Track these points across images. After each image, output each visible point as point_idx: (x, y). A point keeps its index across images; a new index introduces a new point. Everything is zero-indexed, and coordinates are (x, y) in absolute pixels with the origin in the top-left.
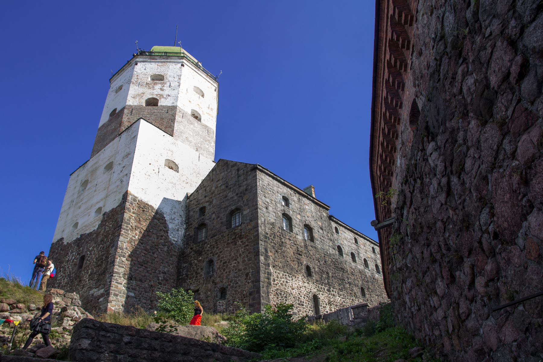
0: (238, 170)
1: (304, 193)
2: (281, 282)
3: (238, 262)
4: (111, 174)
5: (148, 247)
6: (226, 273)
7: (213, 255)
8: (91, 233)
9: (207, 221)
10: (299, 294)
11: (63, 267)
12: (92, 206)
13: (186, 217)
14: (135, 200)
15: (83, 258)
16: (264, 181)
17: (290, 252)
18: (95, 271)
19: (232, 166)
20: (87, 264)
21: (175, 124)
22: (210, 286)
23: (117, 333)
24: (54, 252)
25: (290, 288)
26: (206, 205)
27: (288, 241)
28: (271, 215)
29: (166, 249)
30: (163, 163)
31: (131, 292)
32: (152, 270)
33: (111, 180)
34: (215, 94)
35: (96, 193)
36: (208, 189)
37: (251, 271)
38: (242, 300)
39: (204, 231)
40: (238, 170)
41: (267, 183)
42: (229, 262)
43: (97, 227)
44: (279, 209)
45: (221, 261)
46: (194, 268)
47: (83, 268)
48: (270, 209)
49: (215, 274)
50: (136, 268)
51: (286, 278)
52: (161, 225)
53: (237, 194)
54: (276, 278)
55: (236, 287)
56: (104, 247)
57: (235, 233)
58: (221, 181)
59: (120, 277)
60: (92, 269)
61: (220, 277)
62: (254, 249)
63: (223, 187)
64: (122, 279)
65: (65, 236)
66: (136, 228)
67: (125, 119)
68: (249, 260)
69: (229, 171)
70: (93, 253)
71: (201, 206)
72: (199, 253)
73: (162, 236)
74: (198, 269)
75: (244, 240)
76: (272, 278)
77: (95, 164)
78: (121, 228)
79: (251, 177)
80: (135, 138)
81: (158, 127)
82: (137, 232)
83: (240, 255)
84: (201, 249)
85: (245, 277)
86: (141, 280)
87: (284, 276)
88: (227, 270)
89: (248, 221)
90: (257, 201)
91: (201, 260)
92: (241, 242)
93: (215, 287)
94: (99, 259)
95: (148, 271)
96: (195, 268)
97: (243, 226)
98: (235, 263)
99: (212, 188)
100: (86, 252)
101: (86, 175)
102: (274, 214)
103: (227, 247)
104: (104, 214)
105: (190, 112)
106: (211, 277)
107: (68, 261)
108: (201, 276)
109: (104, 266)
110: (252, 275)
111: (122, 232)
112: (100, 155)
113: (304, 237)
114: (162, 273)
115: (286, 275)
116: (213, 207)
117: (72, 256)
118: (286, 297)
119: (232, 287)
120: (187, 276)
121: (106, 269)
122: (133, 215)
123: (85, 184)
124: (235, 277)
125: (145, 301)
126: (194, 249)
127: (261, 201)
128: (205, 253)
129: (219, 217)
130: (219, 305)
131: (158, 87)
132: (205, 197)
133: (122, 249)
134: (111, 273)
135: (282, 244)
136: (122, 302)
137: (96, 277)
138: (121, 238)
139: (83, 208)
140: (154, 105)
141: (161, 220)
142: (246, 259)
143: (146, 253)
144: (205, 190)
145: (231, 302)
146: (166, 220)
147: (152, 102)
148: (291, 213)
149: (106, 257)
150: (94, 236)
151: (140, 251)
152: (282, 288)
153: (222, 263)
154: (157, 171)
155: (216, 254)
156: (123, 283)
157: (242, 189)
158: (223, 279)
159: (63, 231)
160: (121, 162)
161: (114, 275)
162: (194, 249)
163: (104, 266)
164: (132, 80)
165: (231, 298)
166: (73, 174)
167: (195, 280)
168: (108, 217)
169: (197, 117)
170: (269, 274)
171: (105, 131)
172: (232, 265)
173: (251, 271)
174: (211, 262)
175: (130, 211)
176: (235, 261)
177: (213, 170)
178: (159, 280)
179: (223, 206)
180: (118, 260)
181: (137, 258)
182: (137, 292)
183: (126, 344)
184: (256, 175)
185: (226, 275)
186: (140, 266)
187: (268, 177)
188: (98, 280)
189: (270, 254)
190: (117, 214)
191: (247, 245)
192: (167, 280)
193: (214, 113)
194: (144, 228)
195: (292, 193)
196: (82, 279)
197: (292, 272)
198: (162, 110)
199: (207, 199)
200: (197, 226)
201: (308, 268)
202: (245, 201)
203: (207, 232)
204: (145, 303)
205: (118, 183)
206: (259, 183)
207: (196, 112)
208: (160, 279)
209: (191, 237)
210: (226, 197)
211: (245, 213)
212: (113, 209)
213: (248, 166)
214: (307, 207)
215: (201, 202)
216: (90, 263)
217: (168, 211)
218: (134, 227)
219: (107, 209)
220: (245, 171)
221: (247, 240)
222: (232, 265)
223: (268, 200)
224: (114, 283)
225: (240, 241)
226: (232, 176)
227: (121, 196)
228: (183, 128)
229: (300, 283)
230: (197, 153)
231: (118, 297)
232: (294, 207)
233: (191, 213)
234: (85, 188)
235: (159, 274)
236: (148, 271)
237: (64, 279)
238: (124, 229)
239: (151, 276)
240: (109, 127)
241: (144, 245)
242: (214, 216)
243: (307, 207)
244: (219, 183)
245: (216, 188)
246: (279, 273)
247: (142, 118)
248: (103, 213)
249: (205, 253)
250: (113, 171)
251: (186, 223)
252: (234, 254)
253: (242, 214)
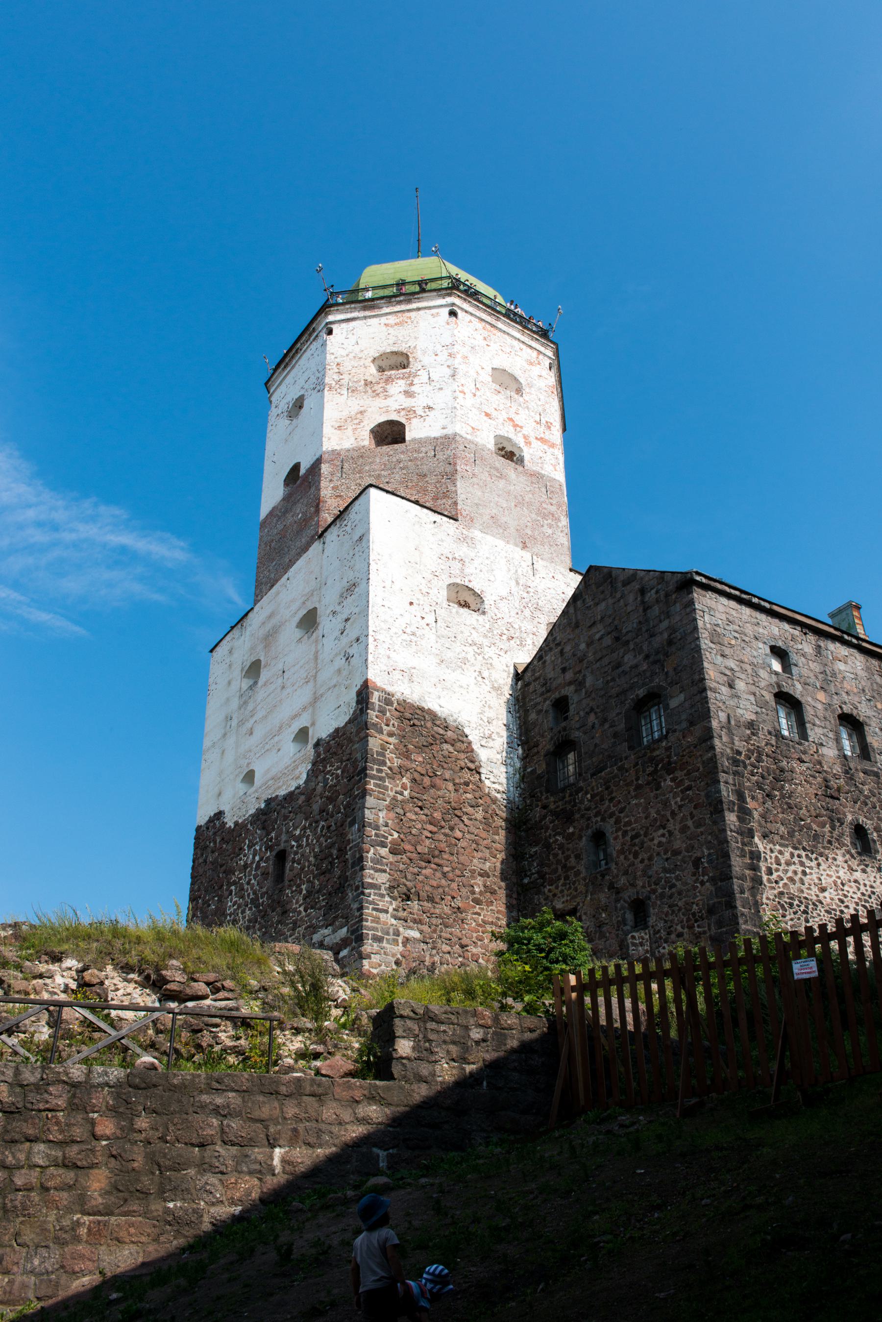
0: (643, 591)
1: (832, 630)
2: (790, 874)
3: (671, 833)
4: (317, 641)
5: (437, 815)
6: (642, 861)
7: (603, 820)
8: (291, 794)
9: (576, 735)
10: (842, 901)
11: (235, 883)
12: (281, 728)
13: (520, 727)
14: (388, 702)
15: (281, 857)
16: (712, 612)
17: (804, 790)
18: (317, 887)
19: (626, 583)
20: (295, 872)
21: (458, 484)
22: (603, 897)
23: (458, 1025)
24: (206, 847)
25: (815, 889)
26: (569, 691)
27: (795, 764)
28: (742, 703)
29: (479, 815)
30: (441, 595)
31: (411, 928)
32: (453, 869)
33: (320, 657)
34: (551, 379)
35: (285, 692)
36: (568, 648)
37: (706, 852)
38: (691, 927)
39: (571, 757)
40: (643, 591)
41: (724, 617)
42: (646, 835)
43: (304, 776)
44: (763, 684)
45: (625, 833)
46: (556, 855)
47: (287, 883)
48: (740, 685)
49: (613, 866)
50: (416, 870)
51: (802, 864)
52: (462, 756)
53: (647, 657)
54: (774, 866)
55: (671, 897)
56: (329, 827)
57: (652, 759)
58: (600, 626)
59: (382, 896)
60: (309, 881)
61: (626, 873)
62: (708, 796)
63: (608, 641)
64: (387, 899)
65: (226, 808)
66: (401, 771)
67: (326, 490)
68: (698, 825)
69: (618, 595)
70: (304, 842)
71: (557, 695)
72: (566, 817)
73: (467, 784)
74: (567, 858)
75: (679, 774)
76: (763, 866)
77: (270, 617)
78: (366, 775)
79: (678, 607)
80: (363, 539)
81: (416, 502)
82: (404, 780)
83: (673, 814)
84: (569, 807)
85: (690, 867)
86: (430, 899)
87: (796, 859)
88: (643, 855)
89: (684, 725)
90: (701, 670)
91: (573, 833)
92: (673, 780)
93: (617, 901)
94: (323, 856)
95: (444, 875)
96: (560, 856)
97: (672, 738)
98: (663, 835)
99: (577, 645)
100: (286, 841)
101: (253, 648)
102: (752, 698)
103: (636, 797)
104: (317, 745)
105: (491, 445)
106: (603, 876)
107: (246, 866)
108: (578, 873)
109: (337, 872)
110: (710, 862)
111: (371, 786)
112: (278, 593)
113: (841, 749)
114: (481, 875)
115: (799, 856)
116: (588, 694)
117: (254, 855)
118: (805, 912)
119: (662, 896)
120: (542, 875)
121: (343, 878)
122: (392, 740)
123: (254, 669)
124: (665, 870)
125: (448, 948)
126: (552, 806)
127: (714, 667)
128: (582, 816)
129: (605, 720)
130: (634, 944)
132: (564, 670)
133: (377, 828)
134: (357, 888)
135: (780, 776)
136: (393, 955)
137: (322, 901)
138: (370, 801)
139: (259, 733)
140: (397, 443)
141: (459, 744)
142: (690, 823)
143: (434, 829)
144: (562, 653)
145: (663, 933)
146: (470, 743)
147: (390, 433)
148: (797, 690)
149: (339, 850)
150: (300, 802)
151: (419, 826)
152: (793, 889)
153: (628, 838)
154: (430, 619)
155: (612, 815)
156: (391, 910)
157: (657, 641)
158: (635, 878)
159: (220, 794)
160: (338, 608)
161: (367, 891)
162: (552, 806)
163: (337, 872)
164: (327, 380)
165: (661, 924)
166: (218, 649)
167: (564, 885)
168: (327, 751)
169: (509, 454)
170: (756, 856)
172: (656, 842)
173: (706, 852)
174: (599, 838)
175: (381, 731)
176: (661, 831)
177: (575, 598)
178: (473, 893)
179: (614, 692)
180: (370, 854)
181: (415, 846)
182: (425, 928)
183: (477, 1043)
184: (692, 602)
185: (641, 866)
186: (423, 864)
187: (724, 600)
188: (330, 908)
189: (751, 804)
190: (350, 740)
191: (689, 788)
192: (493, 892)
193: (556, 434)
194: (419, 769)
195: (797, 633)
196: (288, 907)
197: (816, 846)
198: (419, 452)
199: (569, 675)
200: (550, 747)
201: (859, 831)
202: (671, 673)
203: (579, 761)
204: (449, 953)
205: (340, 662)
206: (704, 622)
207: (509, 440)
208: (477, 890)
209: (539, 777)
210: (618, 665)
211: (674, 703)
212: (337, 730)
213: (667, 577)
214: (841, 666)
215: (554, 685)
216: (302, 869)
217: (474, 719)
218: (396, 770)
219: (324, 728)
220: (662, 593)
221: (688, 774)
222: (656, 842)
223: (732, 664)
224: (368, 911)
225: (668, 778)
226: (629, 609)
227: (351, 697)
228: (479, 493)
229: (841, 874)
230: (527, 555)
231: (385, 944)
232: (805, 672)
233: (533, 716)
234: (256, 683)
235: (473, 877)
236: (444, 875)
237: (243, 912)
238: (373, 777)
239: (454, 885)
240: (289, 516)
241: (426, 811)
242: (592, 718)
243: (841, 666)
244: (594, 630)
245: (588, 645)
246: (781, 852)
247: (371, 485)
248: (312, 741)
249: (582, 816)
250: (319, 632)
251: (523, 744)
252: (658, 812)
253: (666, 707)
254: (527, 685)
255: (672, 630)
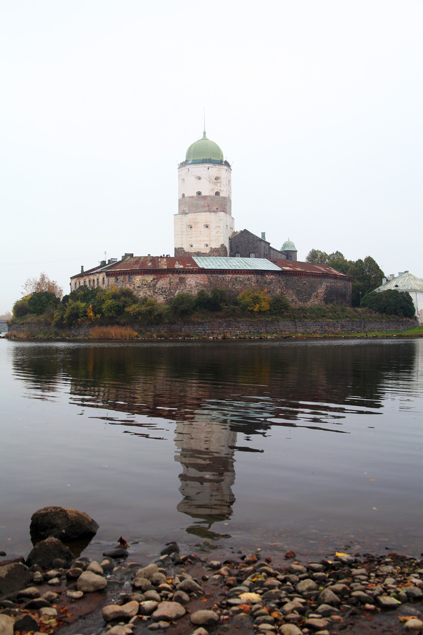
63: (247, 242)
131: (219, 184)
171: (196, 202)
199: (240, 243)
242: (243, 251)
254: (231, 241)
255: (257, 245)
